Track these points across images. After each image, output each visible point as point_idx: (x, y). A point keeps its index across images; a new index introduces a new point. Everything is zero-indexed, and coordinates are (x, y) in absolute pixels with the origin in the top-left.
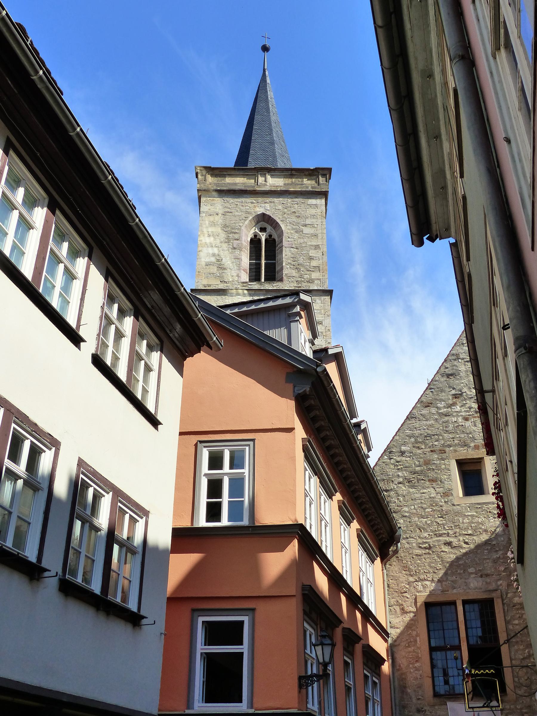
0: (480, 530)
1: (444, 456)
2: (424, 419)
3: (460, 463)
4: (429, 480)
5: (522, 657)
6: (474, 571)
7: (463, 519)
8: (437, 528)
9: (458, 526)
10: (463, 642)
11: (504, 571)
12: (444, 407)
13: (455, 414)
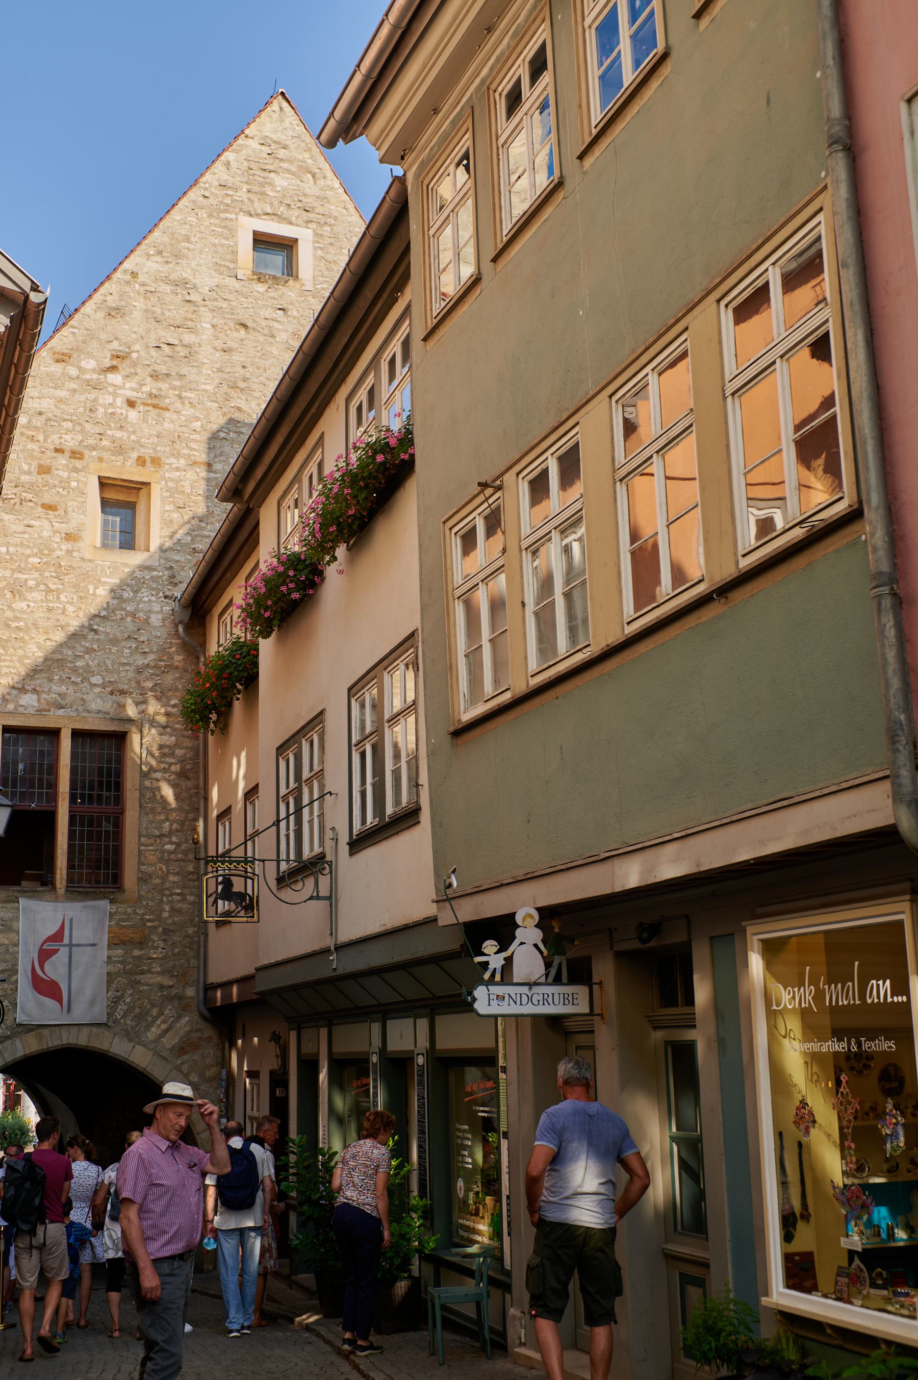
0: (123, 613)
1: (79, 464)
2: (51, 384)
3: (104, 484)
4: (44, 506)
5: (158, 833)
6: (101, 682)
7: (96, 588)
8: (46, 595)
9: (84, 598)
10: (64, 800)
11: (151, 690)
12: (94, 370)
13: (110, 389)
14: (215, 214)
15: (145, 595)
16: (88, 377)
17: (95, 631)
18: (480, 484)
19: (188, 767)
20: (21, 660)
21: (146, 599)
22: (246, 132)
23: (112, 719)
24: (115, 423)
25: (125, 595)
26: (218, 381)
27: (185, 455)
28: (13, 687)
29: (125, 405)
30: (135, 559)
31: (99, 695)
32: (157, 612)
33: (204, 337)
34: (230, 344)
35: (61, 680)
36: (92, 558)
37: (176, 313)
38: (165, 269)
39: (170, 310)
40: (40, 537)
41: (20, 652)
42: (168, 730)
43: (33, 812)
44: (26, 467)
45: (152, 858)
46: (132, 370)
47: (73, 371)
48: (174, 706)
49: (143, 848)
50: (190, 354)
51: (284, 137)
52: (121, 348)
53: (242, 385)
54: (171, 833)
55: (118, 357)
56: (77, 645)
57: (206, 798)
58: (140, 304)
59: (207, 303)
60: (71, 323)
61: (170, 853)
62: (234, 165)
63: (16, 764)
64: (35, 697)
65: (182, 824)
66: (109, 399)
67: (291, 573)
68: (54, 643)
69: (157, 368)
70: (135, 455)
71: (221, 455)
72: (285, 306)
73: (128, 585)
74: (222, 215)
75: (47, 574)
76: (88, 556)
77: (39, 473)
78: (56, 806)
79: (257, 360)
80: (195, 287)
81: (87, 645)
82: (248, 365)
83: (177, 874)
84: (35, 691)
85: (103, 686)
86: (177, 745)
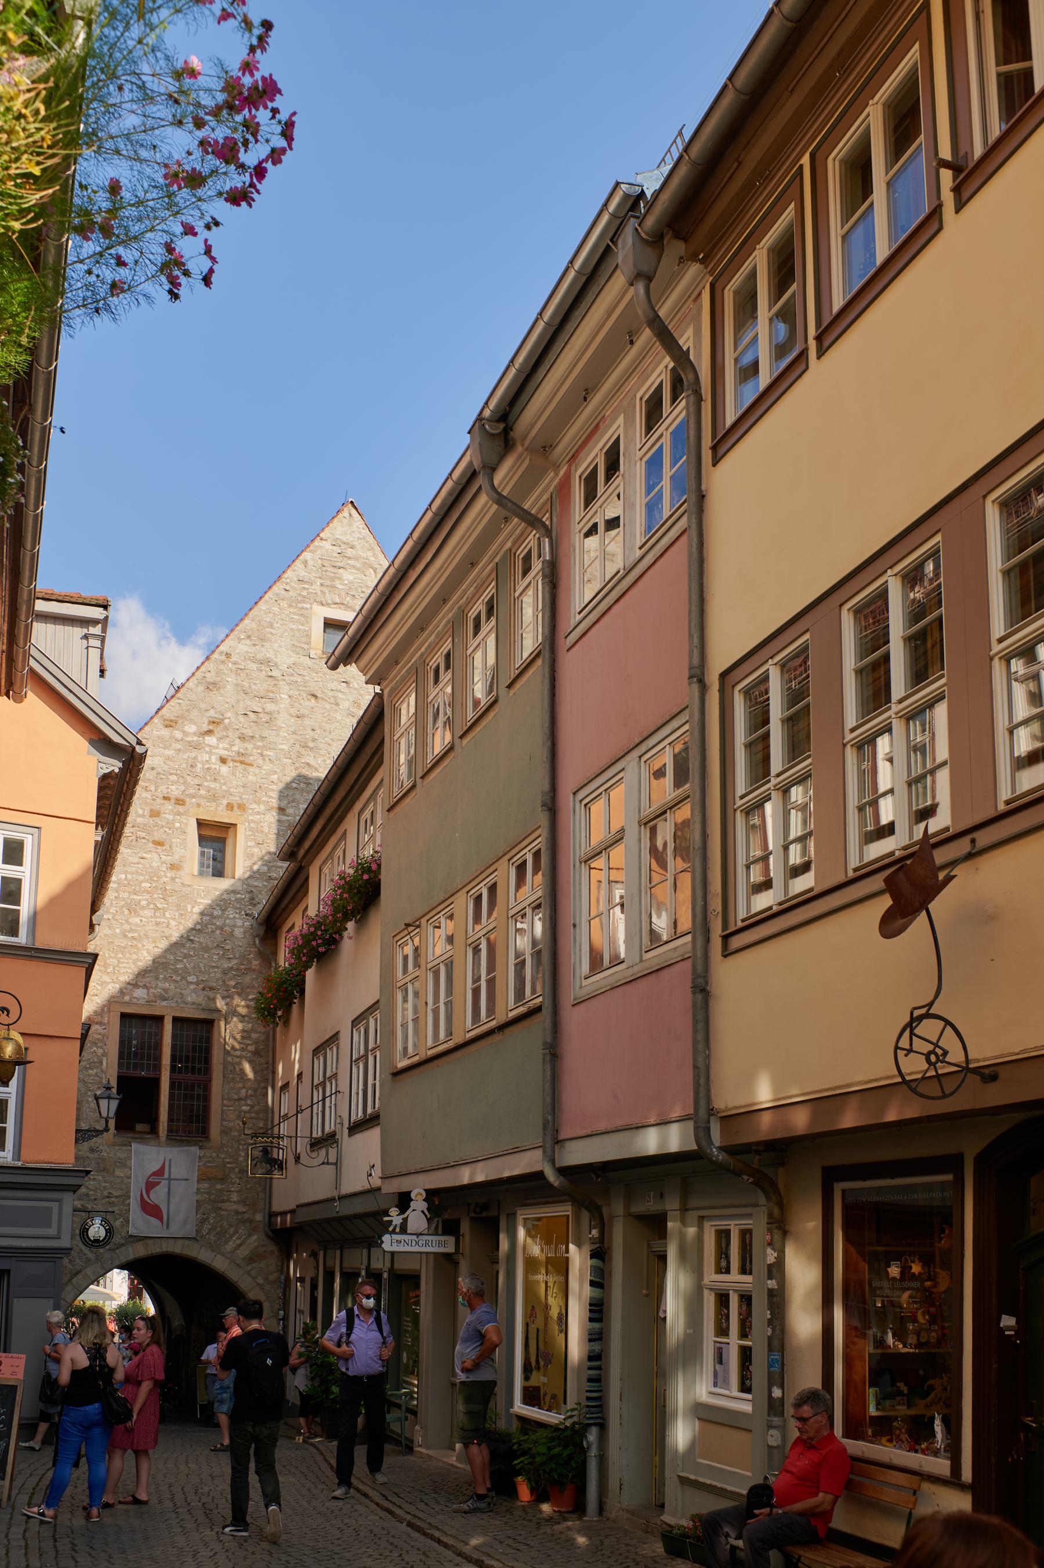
1: (181, 809)
2: (161, 745)
3: (200, 824)
4: (154, 842)
5: (236, 1097)
10: (166, 1070)
11: (234, 987)
13: (207, 749)
14: (294, 604)
15: (231, 913)
16: (190, 739)
17: (192, 941)
18: (406, 925)
19: (261, 1047)
20: (135, 962)
21: (231, 916)
22: (321, 535)
23: (203, 1009)
24: (210, 776)
25: (216, 913)
26: (292, 742)
27: (265, 801)
28: (129, 983)
29: (218, 762)
30: (223, 884)
31: (194, 991)
32: (240, 927)
33: (282, 706)
34: (303, 711)
35: (165, 979)
36: (190, 884)
37: (260, 686)
38: (252, 651)
39: (255, 684)
40: (151, 867)
41: (135, 957)
42: (246, 1018)
43: (143, 1078)
44: (140, 812)
45: (232, 1116)
46: (225, 733)
47: (178, 735)
48: (251, 1000)
49: (225, 1108)
50: (271, 719)
51: (351, 539)
52: (216, 716)
53: (311, 744)
54: (247, 1097)
55: (214, 723)
56: (178, 952)
57: (274, 1072)
58: (231, 679)
59: (286, 678)
60: (178, 695)
61: (245, 1112)
62: (310, 563)
63: (130, 1042)
64: (145, 991)
65: (255, 1091)
66: (206, 757)
67: (319, 933)
68: (160, 950)
69: (244, 731)
70: (225, 802)
71: (293, 802)
72: (348, 679)
73: (218, 905)
74: (299, 605)
75: (155, 896)
76: (187, 882)
77: (150, 816)
78: (160, 1074)
79: (324, 724)
80: (276, 665)
81: (185, 951)
82: (316, 728)
83: (251, 1128)
84: (145, 987)
85: (197, 984)
86: (252, 1030)
